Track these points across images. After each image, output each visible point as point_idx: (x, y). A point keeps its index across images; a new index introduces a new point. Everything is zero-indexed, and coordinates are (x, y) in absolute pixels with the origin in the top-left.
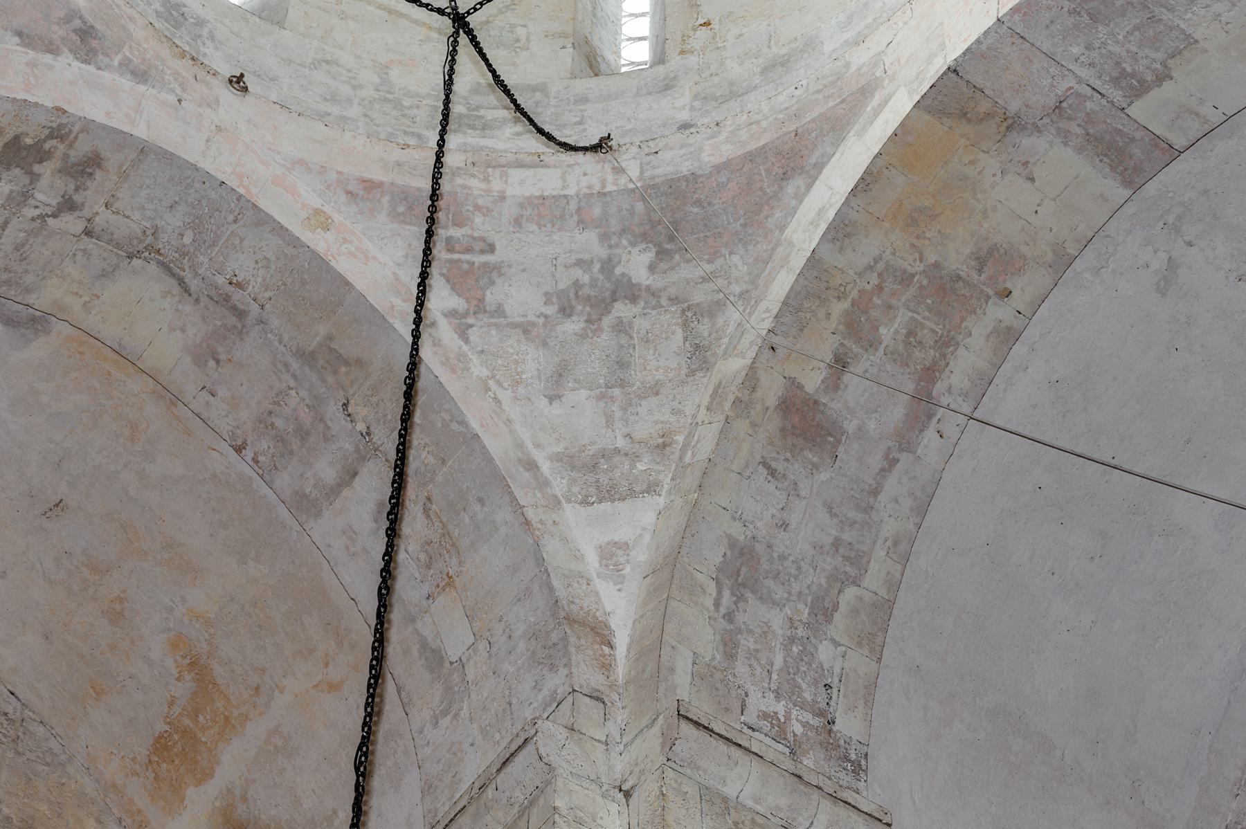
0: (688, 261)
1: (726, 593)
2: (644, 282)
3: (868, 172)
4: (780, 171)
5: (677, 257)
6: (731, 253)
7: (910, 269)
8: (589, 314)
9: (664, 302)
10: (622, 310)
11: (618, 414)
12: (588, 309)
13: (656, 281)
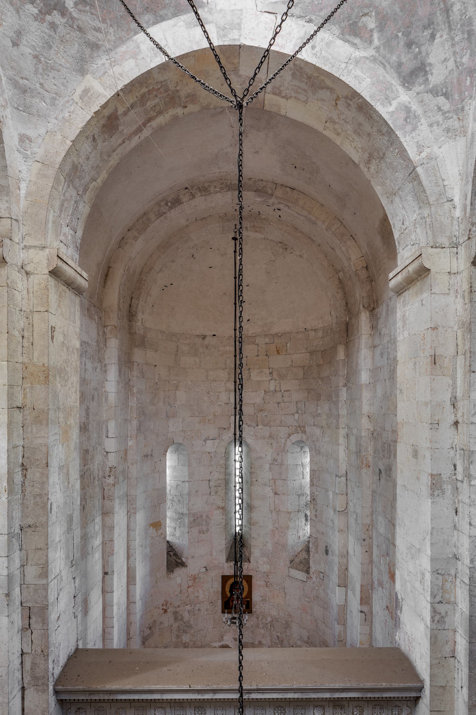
0: (92, 14)
1: (66, 184)
2: (70, 9)
3: (187, 54)
4: (146, 5)
5: (88, 8)
6: (111, 26)
7: (170, 88)
8: (41, 8)
9: (75, 27)
10: (56, 17)
11: (41, 71)
12: (42, 5)
13: (75, 15)
